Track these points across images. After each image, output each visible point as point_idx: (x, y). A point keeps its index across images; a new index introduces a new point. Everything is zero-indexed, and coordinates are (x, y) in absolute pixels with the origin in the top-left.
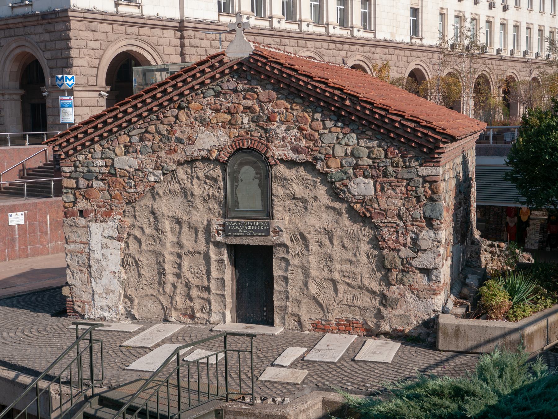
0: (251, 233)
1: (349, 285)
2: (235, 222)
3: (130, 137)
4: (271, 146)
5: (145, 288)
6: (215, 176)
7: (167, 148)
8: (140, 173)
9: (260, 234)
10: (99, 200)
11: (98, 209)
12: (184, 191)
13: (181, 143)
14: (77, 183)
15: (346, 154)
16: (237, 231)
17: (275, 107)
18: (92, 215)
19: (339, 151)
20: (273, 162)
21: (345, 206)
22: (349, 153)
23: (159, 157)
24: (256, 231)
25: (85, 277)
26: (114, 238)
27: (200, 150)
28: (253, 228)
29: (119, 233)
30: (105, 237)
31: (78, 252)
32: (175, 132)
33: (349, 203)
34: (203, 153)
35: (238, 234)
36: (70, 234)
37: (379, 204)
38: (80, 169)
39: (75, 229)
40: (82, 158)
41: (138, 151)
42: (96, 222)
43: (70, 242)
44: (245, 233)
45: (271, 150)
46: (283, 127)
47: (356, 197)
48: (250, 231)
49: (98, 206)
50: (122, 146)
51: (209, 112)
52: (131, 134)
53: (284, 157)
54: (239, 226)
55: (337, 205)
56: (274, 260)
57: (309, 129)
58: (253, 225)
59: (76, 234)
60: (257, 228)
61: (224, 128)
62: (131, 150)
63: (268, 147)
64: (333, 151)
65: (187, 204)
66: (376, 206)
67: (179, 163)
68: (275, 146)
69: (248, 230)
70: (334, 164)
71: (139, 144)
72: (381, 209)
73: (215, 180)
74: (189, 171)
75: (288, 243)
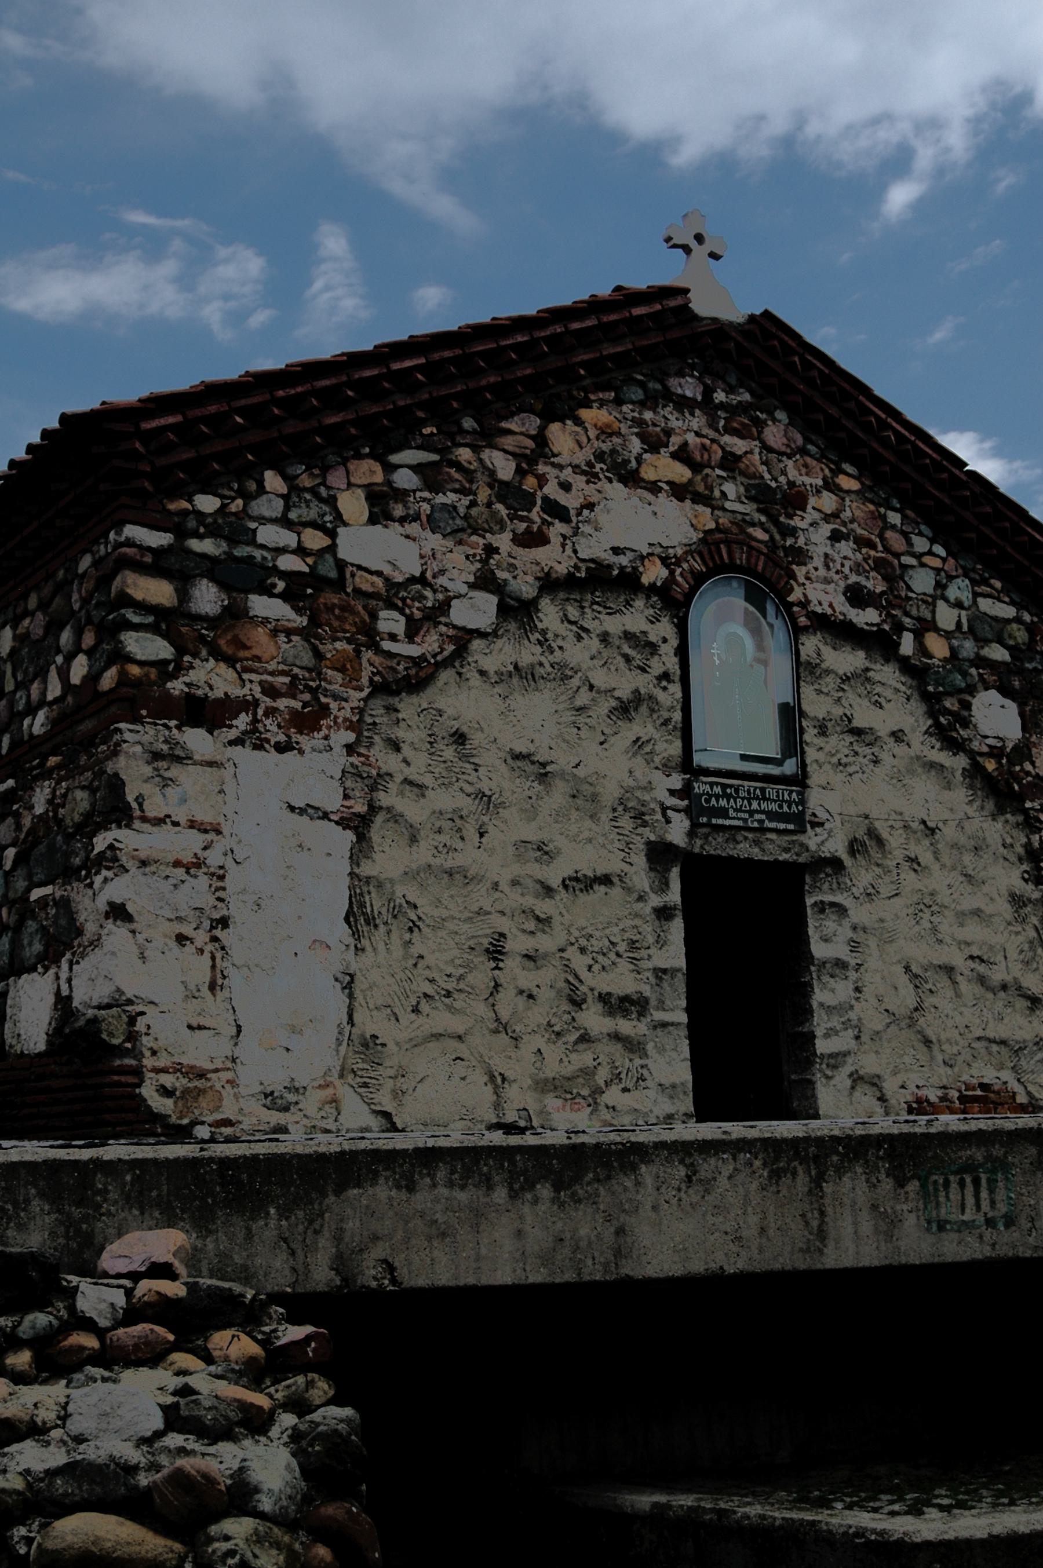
0: (761, 822)
1: (982, 980)
2: (717, 784)
3: (390, 468)
4: (800, 572)
5: (424, 1006)
6: (652, 638)
7: (522, 527)
8: (428, 593)
9: (782, 826)
10: (272, 666)
11: (267, 701)
12: (563, 673)
13: (561, 520)
14: (184, 595)
15: (959, 624)
16: (723, 813)
17: (804, 470)
18: (243, 721)
19: (946, 617)
20: (803, 621)
21: (961, 761)
22: (965, 628)
23: (491, 550)
24: (772, 816)
25: (200, 970)
26: (326, 816)
27: (616, 551)
28: (764, 806)
29: (346, 797)
30: (292, 809)
31: (177, 864)
32: (542, 481)
33: (972, 755)
34: (624, 560)
35: (727, 822)
36: (147, 789)
37: (1033, 763)
38: (206, 546)
39: (176, 771)
40: (208, 503)
41: (424, 518)
42: (258, 747)
43: (144, 819)
44: (745, 820)
45: (799, 585)
46: (826, 529)
47: (989, 741)
48: (757, 816)
49: (271, 691)
50: (360, 493)
51: (636, 445)
52: (395, 458)
53: (829, 611)
54: (729, 797)
55: (943, 758)
56: (809, 911)
57: (880, 548)
58: (765, 799)
59: (169, 791)
60: (774, 807)
61: (681, 499)
62: (398, 511)
63: (793, 576)
64: (933, 612)
65: (568, 717)
66: (1028, 767)
67: (549, 584)
68: (808, 578)
69: (751, 813)
70: (938, 647)
71: (426, 494)
72: (1037, 774)
73: (652, 648)
74: (573, 612)
75: (843, 855)
